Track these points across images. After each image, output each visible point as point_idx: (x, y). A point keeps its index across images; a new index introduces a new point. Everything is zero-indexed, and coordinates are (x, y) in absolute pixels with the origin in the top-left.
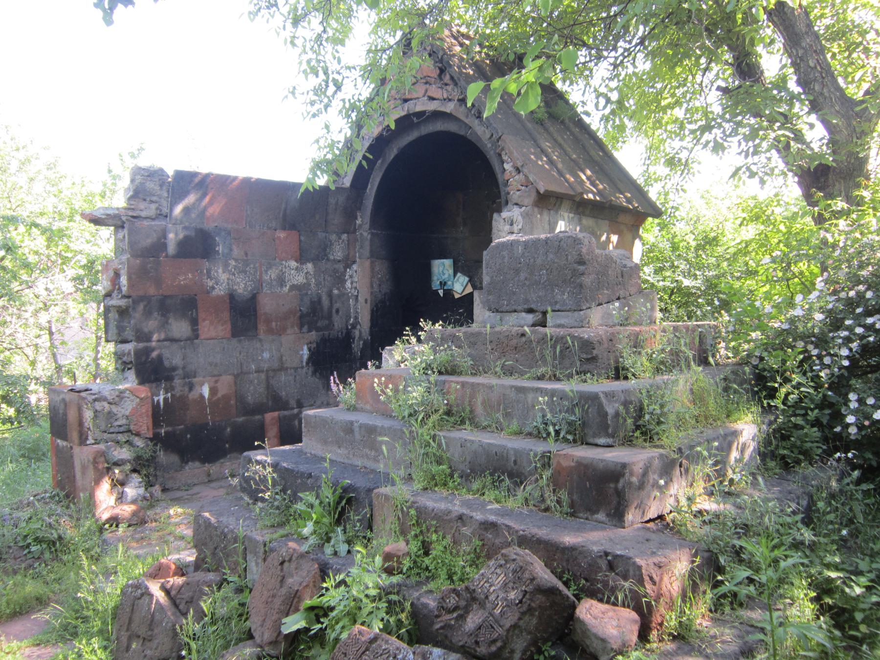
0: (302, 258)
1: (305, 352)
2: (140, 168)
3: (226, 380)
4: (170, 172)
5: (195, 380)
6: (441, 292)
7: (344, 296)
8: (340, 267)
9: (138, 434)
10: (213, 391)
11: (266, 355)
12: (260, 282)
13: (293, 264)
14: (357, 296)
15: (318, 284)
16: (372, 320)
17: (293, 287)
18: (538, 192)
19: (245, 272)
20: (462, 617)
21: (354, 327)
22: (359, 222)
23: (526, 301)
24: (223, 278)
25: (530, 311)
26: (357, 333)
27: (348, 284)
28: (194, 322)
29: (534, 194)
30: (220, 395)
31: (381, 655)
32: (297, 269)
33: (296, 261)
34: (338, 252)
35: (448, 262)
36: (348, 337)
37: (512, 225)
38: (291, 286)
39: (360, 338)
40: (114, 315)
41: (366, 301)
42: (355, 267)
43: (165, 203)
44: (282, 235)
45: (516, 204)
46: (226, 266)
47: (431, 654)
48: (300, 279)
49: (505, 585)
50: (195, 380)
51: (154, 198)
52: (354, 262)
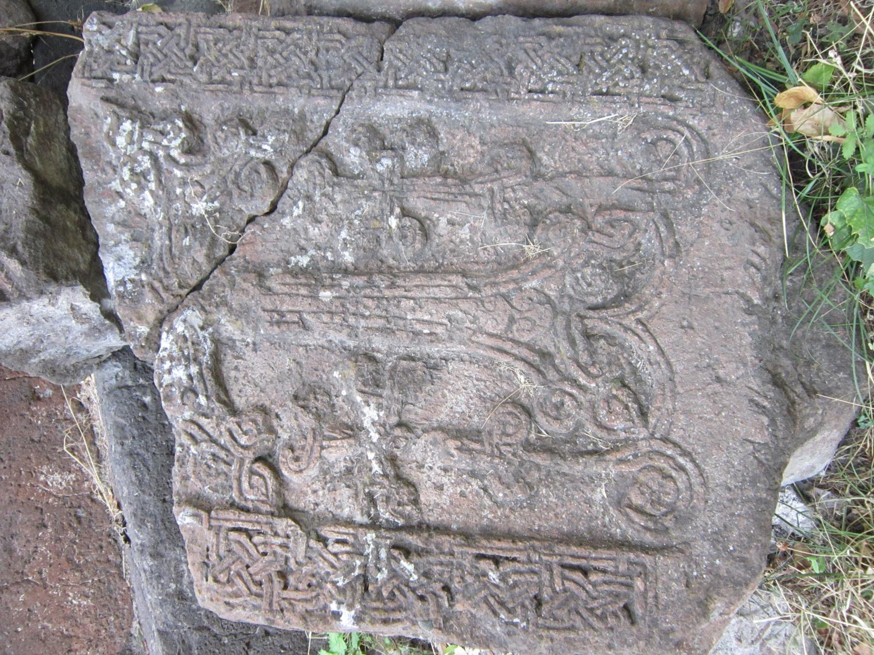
31: (214, 441)
47: (123, 283)
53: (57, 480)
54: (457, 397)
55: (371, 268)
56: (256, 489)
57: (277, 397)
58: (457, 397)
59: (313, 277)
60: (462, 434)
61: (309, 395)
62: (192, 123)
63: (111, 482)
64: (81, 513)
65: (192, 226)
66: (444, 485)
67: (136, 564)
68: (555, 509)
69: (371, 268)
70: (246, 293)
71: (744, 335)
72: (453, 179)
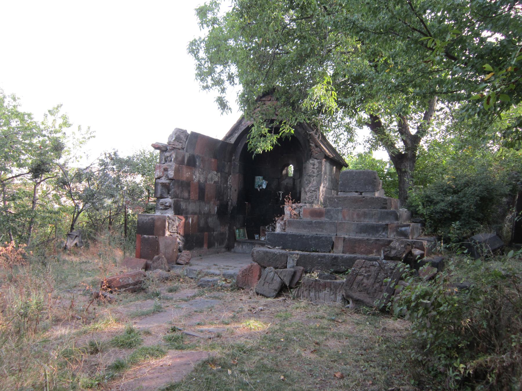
0: (218, 171)
1: (216, 209)
2: (180, 129)
3: (196, 216)
4: (189, 132)
5: (189, 216)
6: (259, 189)
7: (227, 187)
8: (227, 175)
9: (179, 234)
10: (192, 220)
11: (206, 209)
12: (206, 178)
13: (215, 173)
14: (231, 188)
15: (221, 181)
16: (238, 198)
17: (215, 182)
18: (325, 155)
19: (203, 174)
20: (390, 252)
21: (229, 200)
22: (234, 158)
23: (356, 189)
24: (197, 176)
25: (357, 192)
26: (230, 203)
27: (228, 183)
28: (189, 192)
29: (324, 156)
30: (194, 222)
32: (216, 175)
33: (216, 171)
34: (227, 170)
35: (261, 177)
36: (227, 204)
37: (314, 165)
38: (215, 182)
39: (231, 205)
40: (159, 187)
41: (236, 190)
42: (231, 176)
43: (184, 144)
44: (213, 160)
45: (316, 159)
46: (199, 170)
48: (216, 179)
49: (399, 245)
50: (189, 216)
51: (182, 141)
52: (231, 174)
53: (375, 251)
54: (365, 281)
55: (377, 277)
56: (364, 266)
57: (370, 269)
58: (365, 281)
59: (378, 274)
60: (362, 280)
61: (369, 271)
62: (393, 269)
63: (371, 256)
64: (371, 252)
65: (385, 267)
66: (359, 278)
67: (364, 256)
68: (355, 284)
69: (377, 277)
70: (378, 269)
71: (362, 299)
72: (381, 286)
